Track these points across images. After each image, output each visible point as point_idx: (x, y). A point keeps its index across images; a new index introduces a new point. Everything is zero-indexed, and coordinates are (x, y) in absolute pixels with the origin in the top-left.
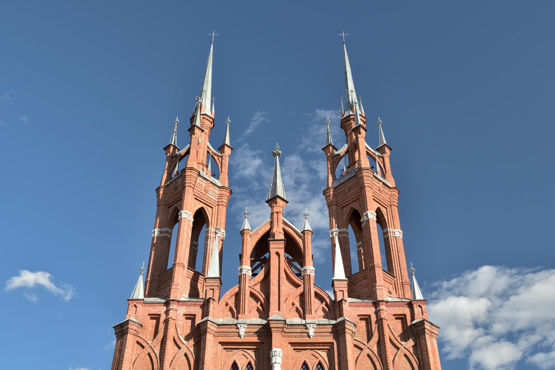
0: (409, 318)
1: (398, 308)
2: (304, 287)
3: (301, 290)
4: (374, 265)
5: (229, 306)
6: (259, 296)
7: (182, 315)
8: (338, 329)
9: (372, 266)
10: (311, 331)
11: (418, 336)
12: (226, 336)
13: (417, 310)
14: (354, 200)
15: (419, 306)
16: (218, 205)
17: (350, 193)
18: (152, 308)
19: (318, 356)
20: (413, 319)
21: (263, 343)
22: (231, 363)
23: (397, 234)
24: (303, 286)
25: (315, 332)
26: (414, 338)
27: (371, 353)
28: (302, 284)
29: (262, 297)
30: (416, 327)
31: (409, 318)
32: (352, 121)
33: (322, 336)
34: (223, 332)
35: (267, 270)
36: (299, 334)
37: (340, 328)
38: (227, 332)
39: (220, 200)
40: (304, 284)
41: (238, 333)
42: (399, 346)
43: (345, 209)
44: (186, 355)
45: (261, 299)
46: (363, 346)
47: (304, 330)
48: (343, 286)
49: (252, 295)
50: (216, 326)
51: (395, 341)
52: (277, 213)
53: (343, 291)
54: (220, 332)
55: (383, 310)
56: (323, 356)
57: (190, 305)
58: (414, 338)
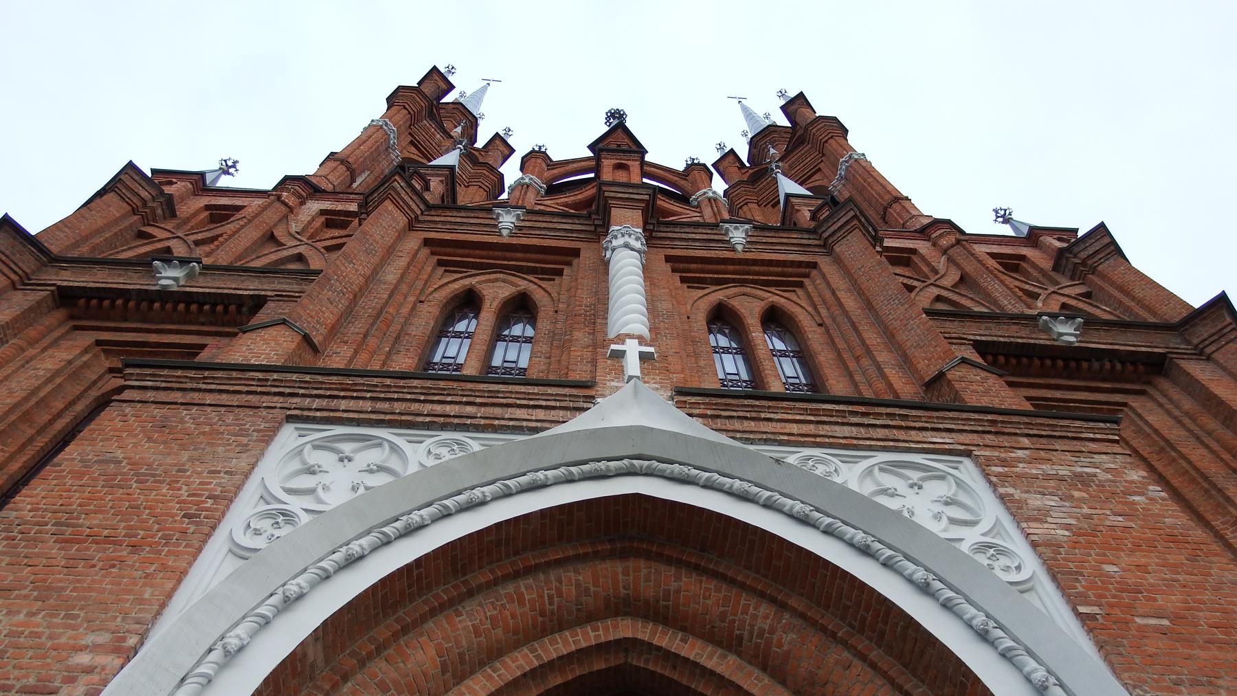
11: (1094, 271)
12: (450, 231)
46: (915, 283)
50: (422, 206)
54: (436, 222)
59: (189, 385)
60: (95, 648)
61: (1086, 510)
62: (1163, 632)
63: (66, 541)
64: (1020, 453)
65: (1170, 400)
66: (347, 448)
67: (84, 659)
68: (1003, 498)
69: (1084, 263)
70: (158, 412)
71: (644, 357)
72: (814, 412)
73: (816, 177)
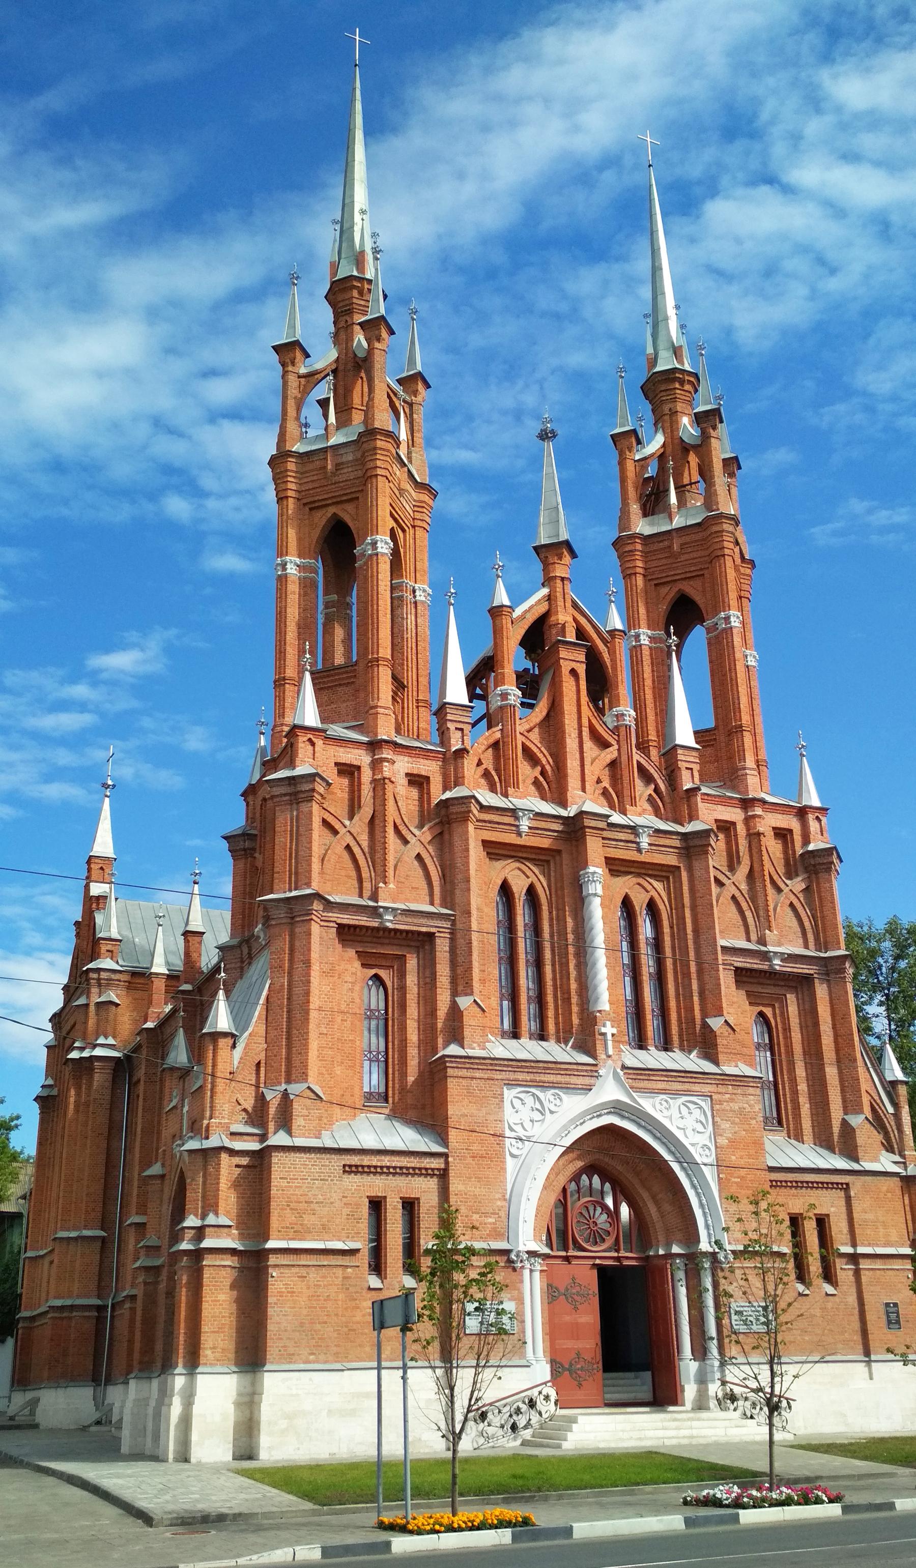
0: (798, 838)
1: (780, 816)
2: (619, 750)
3: (611, 754)
4: (741, 726)
5: (484, 766)
6: (540, 755)
7: (402, 774)
8: (691, 843)
9: (736, 727)
10: (644, 841)
11: (816, 873)
12: (494, 830)
13: (813, 826)
14: (688, 575)
15: (817, 818)
16: (414, 527)
17: (683, 558)
18: (342, 749)
19: (649, 887)
20: (806, 840)
21: (559, 852)
22: (500, 883)
23: (752, 662)
24: (616, 747)
25: (650, 844)
26: (806, 876)
27: (738, 894)
28: (614, 742)
29: (545, 758)
30: (814, 857)
31: (798, 838)
32: (677, 386)
33: (661, 852)
34: (490, 822)
35: (551, 701)
36: (622, 844)
37: (697, 842)
38: (498, 823)
39: (418, 516)
40: (618, 742)
41: (517, 826)
42: (782, 886)
43: (664, 590)
44: (419, 857)
45: (544, 761)
47: (631, 837)
48: (692, 759)
49: (528, 753)
51: (775, 877)
52: (563, 579)
53: (691, 769)
54: (485, 821)
55: (759, 816)
56: (659, 890)
57: (417, 756)
58: (806, 876)
59: (468, 1066)
60: (500, 1199)
61: (737, 1129)
62: (736, 1183)
63: (473, 1157)
64: (727, 1096)
65: (803, 999)
66: (522, 1096)
67: (499, 1203)
68: (714, 1123)
69: (814, 866)
70: (464, 1082)
71: (613, 1035)
72: (666, 1076)
73: (697, 583)
